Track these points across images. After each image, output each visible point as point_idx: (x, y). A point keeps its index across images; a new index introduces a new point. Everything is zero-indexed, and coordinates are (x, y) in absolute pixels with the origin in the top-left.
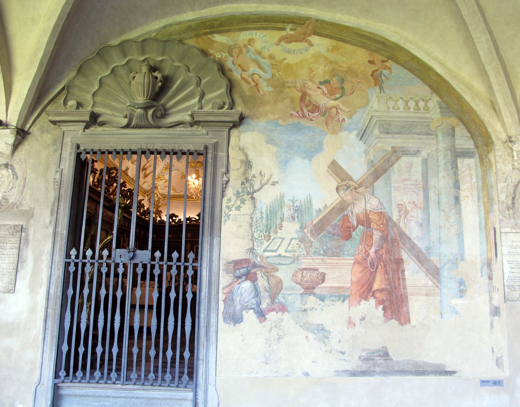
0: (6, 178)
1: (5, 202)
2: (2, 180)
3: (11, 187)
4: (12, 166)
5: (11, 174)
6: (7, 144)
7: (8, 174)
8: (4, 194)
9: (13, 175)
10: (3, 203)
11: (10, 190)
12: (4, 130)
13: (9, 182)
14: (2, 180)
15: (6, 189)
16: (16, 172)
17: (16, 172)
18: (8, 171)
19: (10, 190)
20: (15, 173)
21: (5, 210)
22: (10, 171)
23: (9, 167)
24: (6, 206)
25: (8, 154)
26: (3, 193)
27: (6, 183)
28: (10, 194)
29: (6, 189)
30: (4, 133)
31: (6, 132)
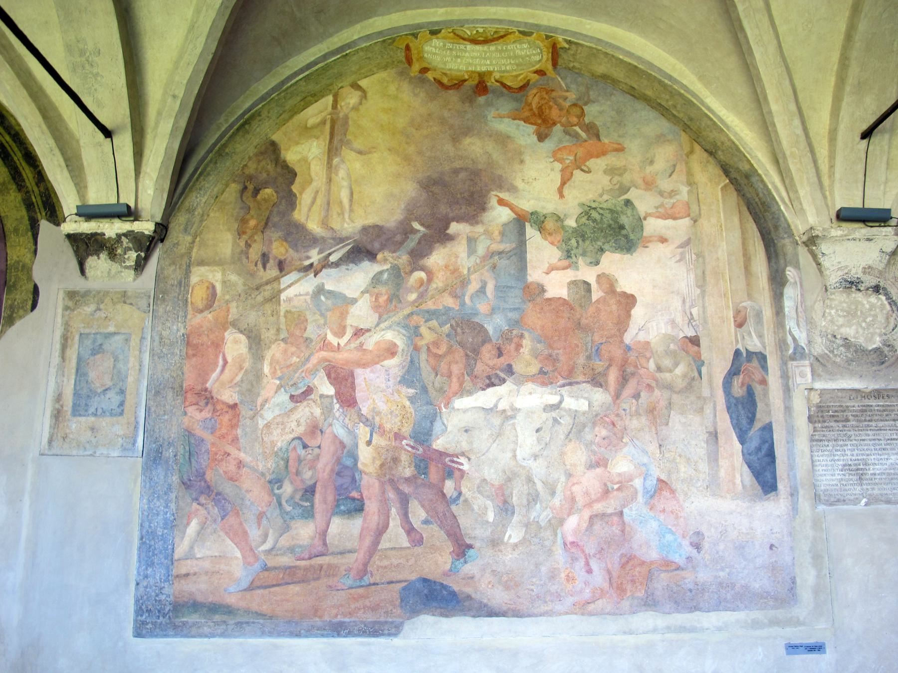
0: (878, 310)
1: (890, 351)
2: (872, 313)
3: (892, 326)
4: (884, 289)
5: (886, 302)
6: (883, 252)
7: (879, 303)
8: (885, 337)
9: (890, 304)
10: (886, 352)
11: (893, 330)
12: (881, 229)
13: (885, 316)
14: (872, 313)
15: (885, 328)
16: (894, 299)
17: (894, 299)
18: (880, 299)
19: (893, 330)
20: (893, 301)
21: (893, 363)
22: (883, 298)
23: (881, 291)
24: (892, 357)
25: (880, 269)
26: (880, 335)
27: (881, 318)
28: (895, 338)
29: (885, 328)
30: (884, 234)
31: (886, 232)
